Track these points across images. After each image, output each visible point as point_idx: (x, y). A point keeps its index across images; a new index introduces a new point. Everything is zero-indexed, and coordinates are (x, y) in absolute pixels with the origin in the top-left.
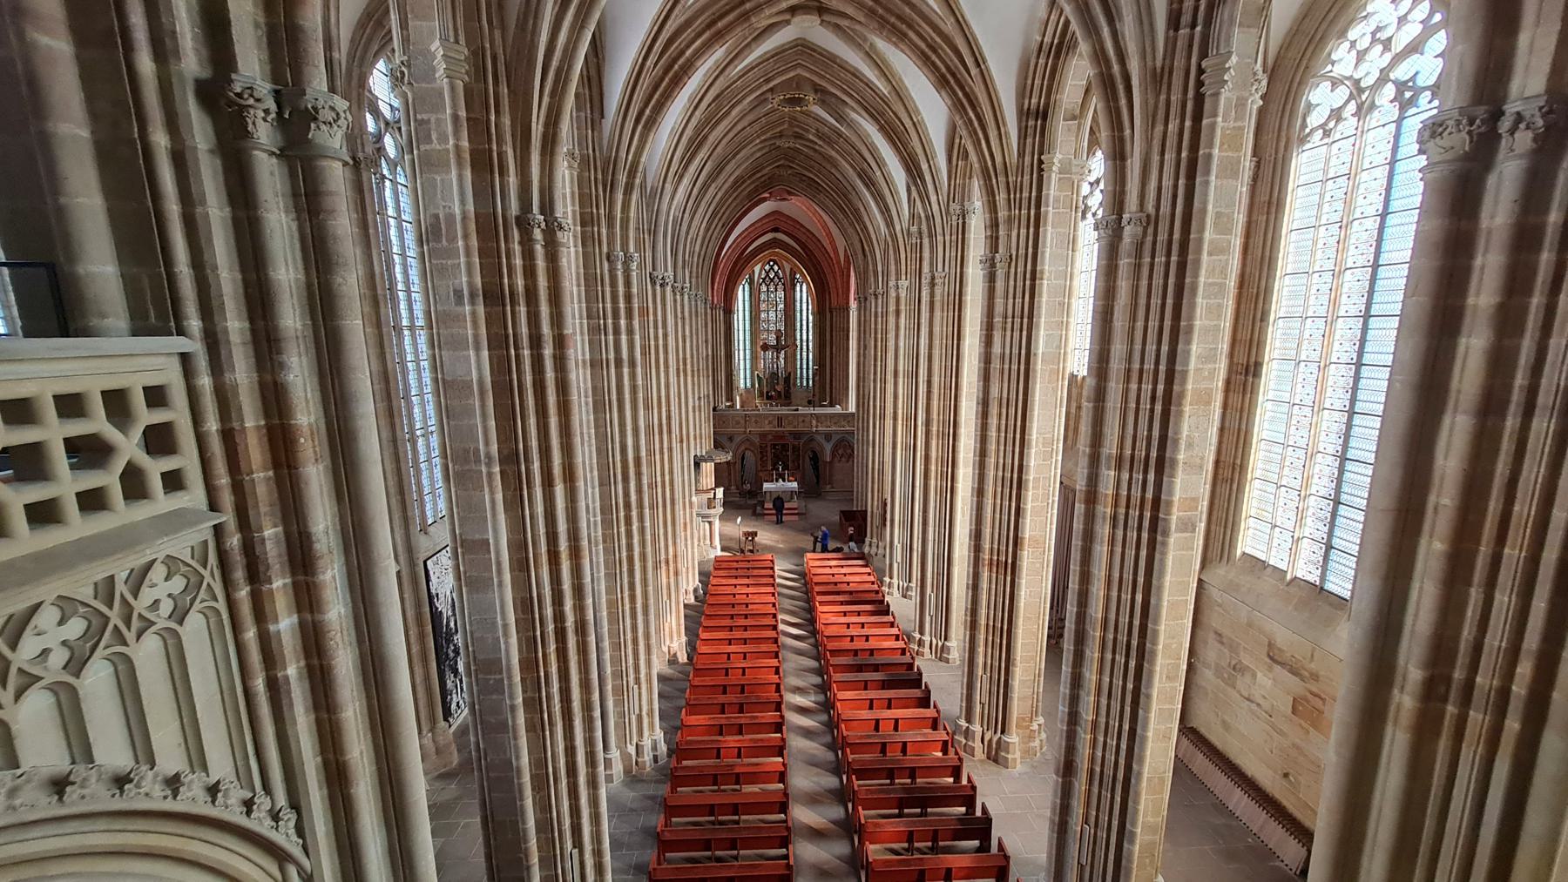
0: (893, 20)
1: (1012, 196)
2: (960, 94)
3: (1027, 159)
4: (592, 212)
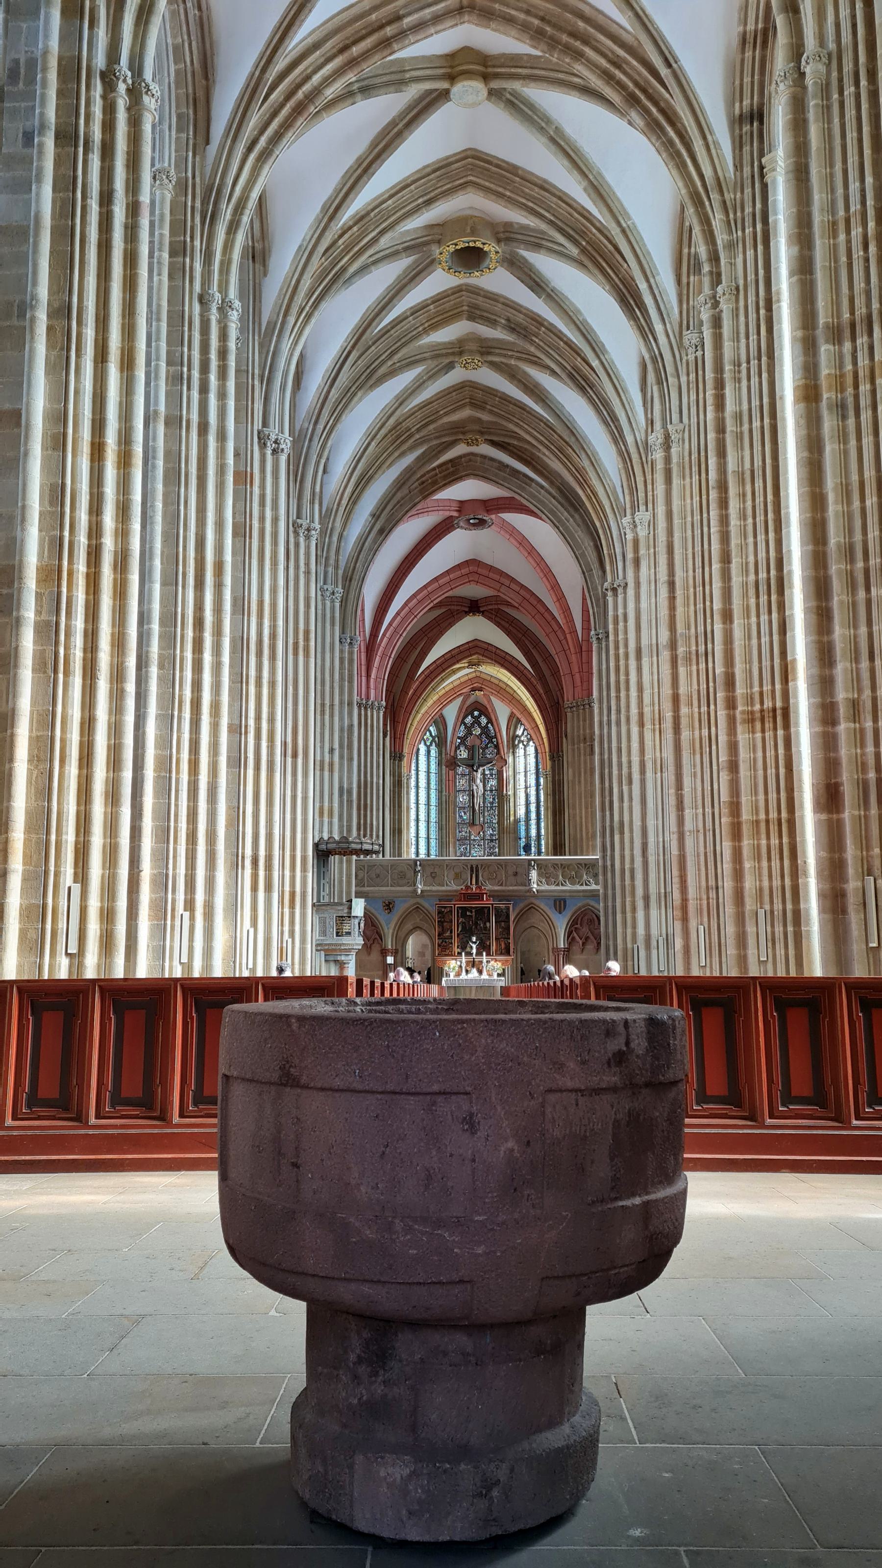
0: (565, 38)
2: (654, 110)
3: (747, 170)
4: (185, 242)
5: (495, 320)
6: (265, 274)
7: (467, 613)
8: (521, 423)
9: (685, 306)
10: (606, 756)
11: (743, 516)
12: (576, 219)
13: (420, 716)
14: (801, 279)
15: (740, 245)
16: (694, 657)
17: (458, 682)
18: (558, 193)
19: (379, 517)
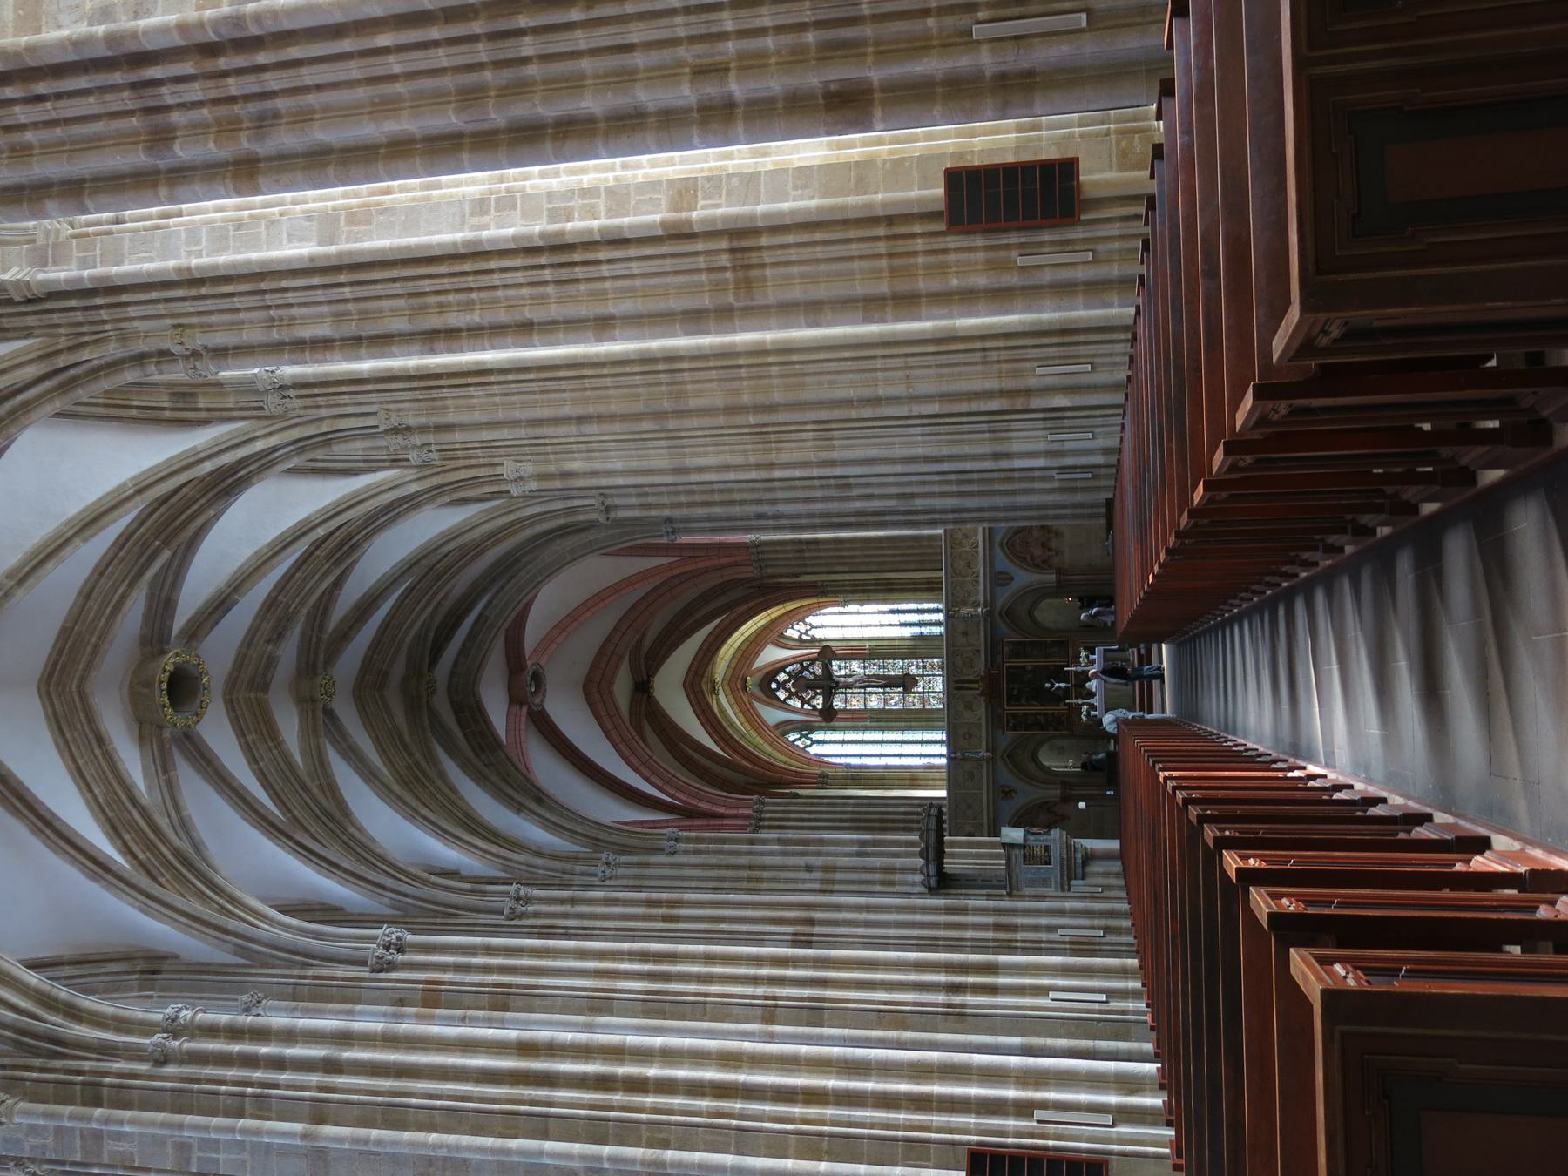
1: (86, 339)
4: (84, 1084)
5: (269, 658)
6: (176, 957)
7: (650, 696)
8: (405, 627)
9: (235, 414)
10: (817, 521)
11: (469, 306)
12: (128, 553)
13: (775, 753)
14: (90, 194)
15: (123, 325)
16: (676, 388)
17: (735, 706)
18: (95, 577)
19: (520, 803)
